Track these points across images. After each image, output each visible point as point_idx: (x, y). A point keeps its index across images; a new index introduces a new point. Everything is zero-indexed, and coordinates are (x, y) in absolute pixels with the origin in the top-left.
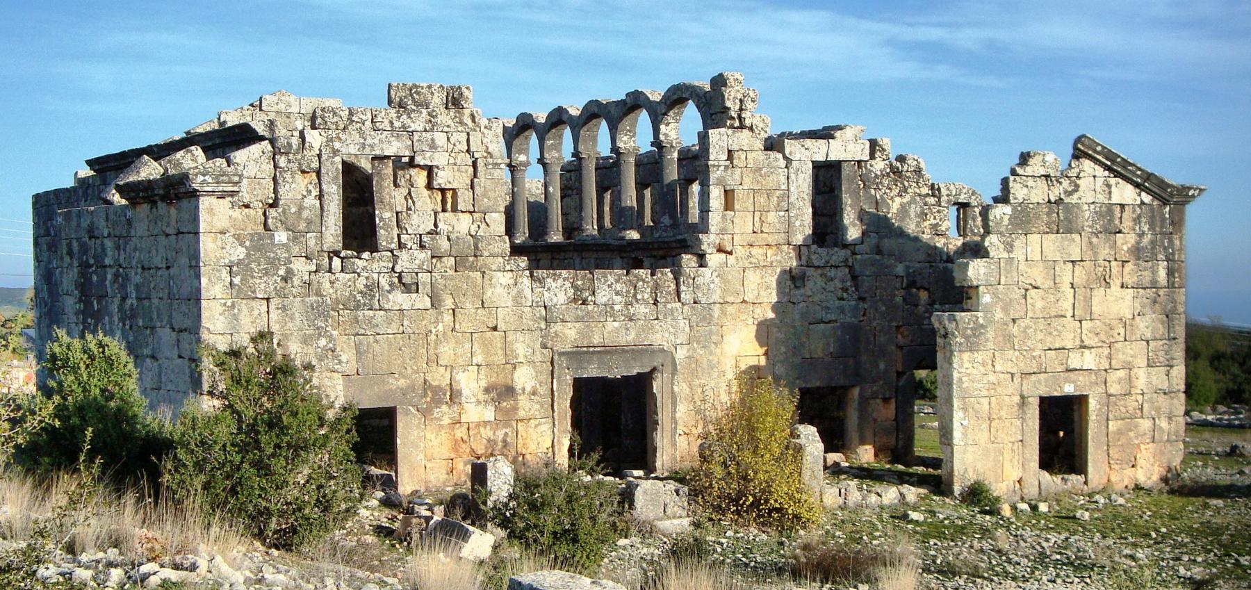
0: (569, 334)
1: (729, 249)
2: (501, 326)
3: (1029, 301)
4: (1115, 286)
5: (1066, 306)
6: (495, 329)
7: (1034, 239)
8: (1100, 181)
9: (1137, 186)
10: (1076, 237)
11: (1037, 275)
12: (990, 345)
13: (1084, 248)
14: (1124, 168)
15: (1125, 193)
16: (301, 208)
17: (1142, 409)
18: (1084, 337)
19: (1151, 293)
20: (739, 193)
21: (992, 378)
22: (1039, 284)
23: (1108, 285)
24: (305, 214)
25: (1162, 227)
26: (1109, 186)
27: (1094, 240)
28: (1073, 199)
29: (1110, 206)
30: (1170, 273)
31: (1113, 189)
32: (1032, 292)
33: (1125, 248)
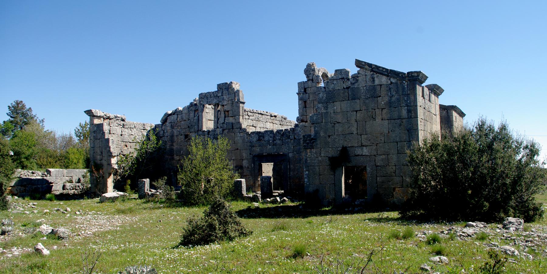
0: (257, 150)
1: (305, 120)
2: (239, 148)
3: (336, 128)
4: (378, 120)
5: (354, 130)
6: (238, 149)
7: (337, 104)
8: (369, 77)
9: (388, 76)
10: (358, 101)
11: (339, 118)
12: (319, 146)
13: (361, 105)
14: (378, 69)
15: (384, 80)
16: (194, 120)
17: (395, 172)
18: (363, 142)
19: (398, 121)
20: (308, 102)
21: (320, 158)
22: (340, 121)
23: (374, 119)
24: (195, 121)
25: (403, 92)
26: (373, 78)
27: (367, 101)
28: (356, 86)
29: (374, 88)
30: (409, 111)
31: (376, 79)
32: (337, 125)
33: (383, 103)
